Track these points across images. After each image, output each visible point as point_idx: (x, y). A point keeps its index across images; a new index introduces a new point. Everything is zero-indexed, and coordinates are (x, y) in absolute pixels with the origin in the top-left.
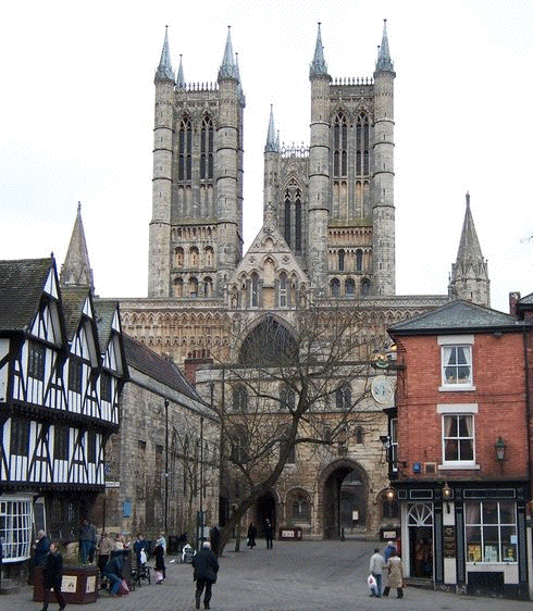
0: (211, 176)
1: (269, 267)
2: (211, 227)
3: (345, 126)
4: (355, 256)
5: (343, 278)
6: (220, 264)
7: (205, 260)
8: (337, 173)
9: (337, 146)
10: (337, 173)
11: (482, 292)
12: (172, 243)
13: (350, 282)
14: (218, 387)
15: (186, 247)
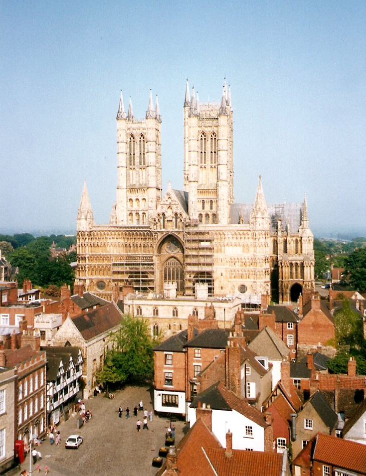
0: (144, 164)
1: (169, 210)
2: (145, 189)
3: (205, 139)
4: (210, 203)
5: (204, 214)
6: (149, 207)
7: (142, 205)
8: (201, 162)
9: (202, 149)
10: (201, 162)
11: (265, 223)
12: (127, 198)
13: (207, 215)
14: (131, 307)
15: (134, 199)
